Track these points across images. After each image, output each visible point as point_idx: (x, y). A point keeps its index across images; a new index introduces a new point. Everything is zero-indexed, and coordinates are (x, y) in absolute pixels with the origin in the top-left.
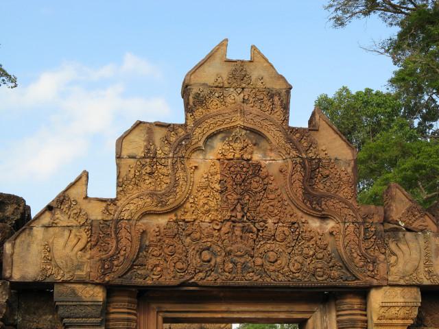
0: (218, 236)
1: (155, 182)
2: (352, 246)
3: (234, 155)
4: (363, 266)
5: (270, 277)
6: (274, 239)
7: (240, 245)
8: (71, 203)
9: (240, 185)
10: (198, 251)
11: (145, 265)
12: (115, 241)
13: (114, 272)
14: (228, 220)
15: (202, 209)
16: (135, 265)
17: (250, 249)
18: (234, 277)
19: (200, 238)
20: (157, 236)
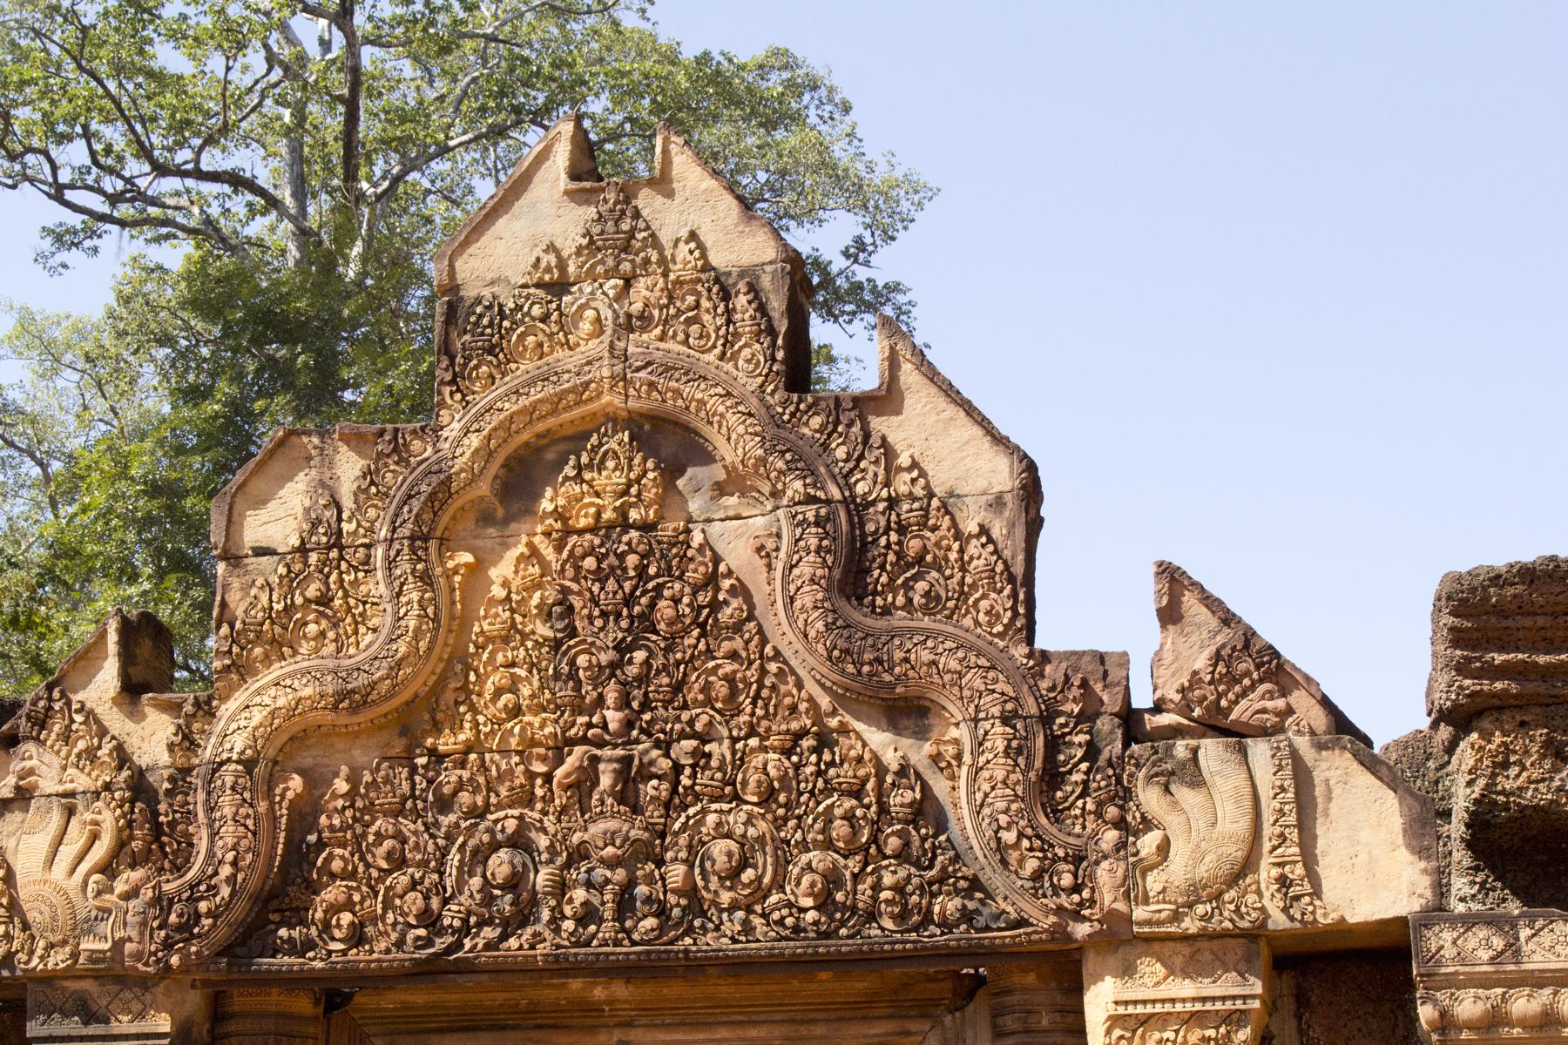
0: (543, 798)
1: (335, 626)
2: (1001, 805)
3: (598, 515)
4: (1037, 876)
6: (737, 798)
7: (612, 824)
8: (72, 721)
9: (618, 615)
10: (475, 852)
11: (307, 910)
12: (204, 833)
13: (199, 936)
14: (584, 740)
16: (275, 911)
18: (594, 936)
20: (344, 808)
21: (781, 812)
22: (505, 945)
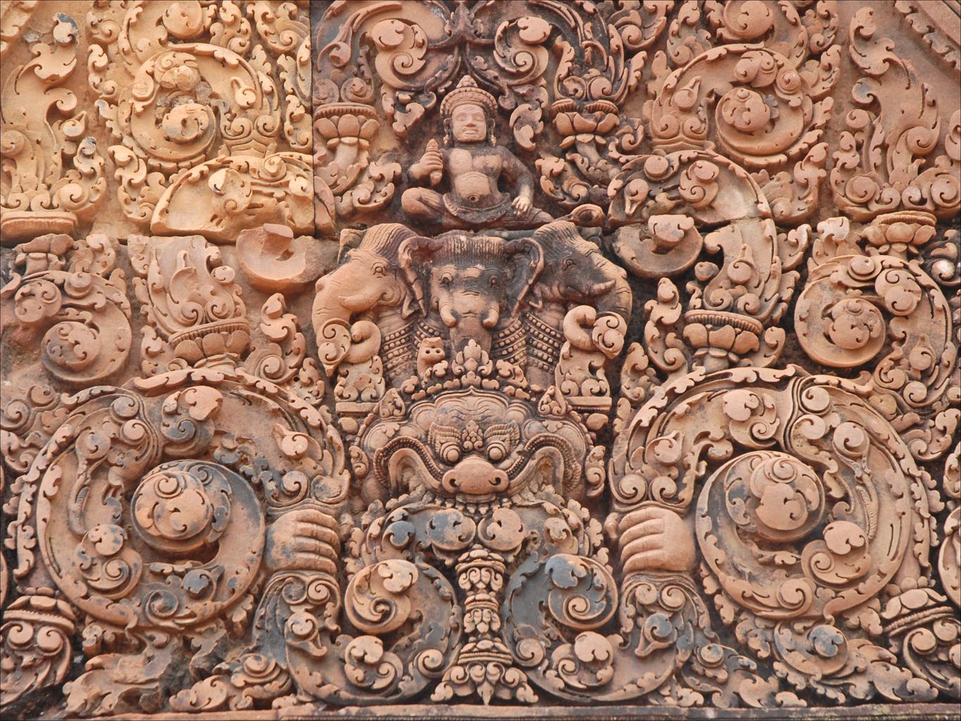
0: (283, 342)
5: (766, 667)
10: (100, 466)
15: (146, 132)
17: (571, 434)
19: (132, 364)
21: (917, 390)
22: (188, 696)
